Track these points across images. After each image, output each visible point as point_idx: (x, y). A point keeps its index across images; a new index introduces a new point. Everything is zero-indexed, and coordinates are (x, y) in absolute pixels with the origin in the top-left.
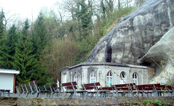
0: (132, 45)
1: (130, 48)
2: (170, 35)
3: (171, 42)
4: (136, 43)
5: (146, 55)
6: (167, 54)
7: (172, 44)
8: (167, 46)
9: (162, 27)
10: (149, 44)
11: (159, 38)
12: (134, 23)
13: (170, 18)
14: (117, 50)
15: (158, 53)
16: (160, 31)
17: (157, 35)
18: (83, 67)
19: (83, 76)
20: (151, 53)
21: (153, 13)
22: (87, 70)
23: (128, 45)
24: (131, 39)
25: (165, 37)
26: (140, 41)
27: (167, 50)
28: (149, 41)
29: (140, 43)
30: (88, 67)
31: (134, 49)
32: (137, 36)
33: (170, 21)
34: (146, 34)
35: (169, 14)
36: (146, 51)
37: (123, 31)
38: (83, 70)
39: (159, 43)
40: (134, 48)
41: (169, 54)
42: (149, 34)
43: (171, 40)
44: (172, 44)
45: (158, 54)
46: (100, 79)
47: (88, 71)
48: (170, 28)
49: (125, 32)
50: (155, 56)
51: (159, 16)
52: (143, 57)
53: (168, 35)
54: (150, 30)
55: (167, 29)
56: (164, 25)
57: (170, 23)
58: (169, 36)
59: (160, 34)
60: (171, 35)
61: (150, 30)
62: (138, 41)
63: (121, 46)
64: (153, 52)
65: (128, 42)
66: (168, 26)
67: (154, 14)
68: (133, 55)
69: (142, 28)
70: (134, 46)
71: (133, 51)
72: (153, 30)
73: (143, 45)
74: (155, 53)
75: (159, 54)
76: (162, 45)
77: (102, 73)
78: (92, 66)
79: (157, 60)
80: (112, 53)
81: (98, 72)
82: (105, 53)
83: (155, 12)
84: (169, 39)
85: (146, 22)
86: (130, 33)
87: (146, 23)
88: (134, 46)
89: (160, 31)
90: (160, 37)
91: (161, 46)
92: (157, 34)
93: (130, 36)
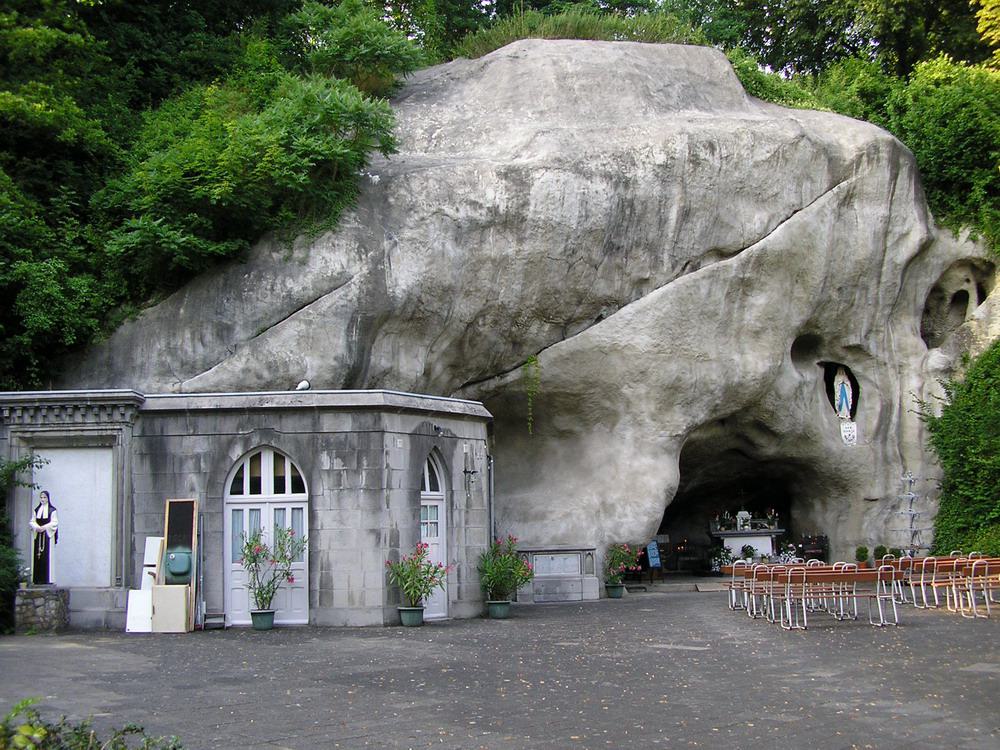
0: (482, 314)
1: (462, 326)
2: (660, 310)
3: (659, 345)
4: (503, 306)
5: (512, 376)
6: (626, 390)
7: (659, 352)
8: (637, 357)
9: (631, 263)
10: (547, 327)
11: (598, 309)
12: (533, 202)
13: (671, 235)
14: (404, 326)
15: (577, 380)
16: (617, 277)
17: (600, 295)
18: (387, 420)
19: (389, 487)
20: (547, 376)
21: (616, 185)
22: (408, 448)
23: (464, 308)
24: (493, 279)
25: (638, 312)
26: (528, 303)
27: (632, 374)
28: (557, 313)
29: (519, 314)
30: (414, 422)
31: (480, 334)
32: (527, 274)
33: (667, 247)
34: (566, 278)
35: (673, 215)
36: (520, 360)
37: (465, 226)
38: (388, 438)
39: (599, 333)
40: (481, 329)
41: (638, 397)
42: (576, 282)
43: (661, 333)
44: (659, 352)
45: (576, 384)
46: (468, 505)
47: (411, 450)
48: (660, 278)
49: (470, 230)
50: (555, 391)
51: (639, 208)
52: (492, 384)
53: (654, 306)
55: (646, 280)
56: (643, 256)
57: (666, 257)
58: (657, 313)
59: (609, 293)
60: (664, 310)
62: (522, 299)
63: (436, 305)
64: (556, 371)
65: (468, 294)
66: (656, 264)
67: (621, 189)
68: (453, 366)
69: (567, 240)
70: (489, 319)
71: (467, 345)
73: (526, 325)
74: (564, 376)
75: (582, 386)
76: (614, 349)
77: (477, 469)
78: (429, 419)
80: (378, 338)
81: (458, 466)
82: (349, 330)
83: (627, 184)
84: (654, 327)
85: (587, 217)
86: (497, 245)
87: (587, 225)
88: (489, 319)
89: (617, 277)
90: (608, 305)
91: (604, 352)
92: (602, 289)
93: (494, 261)
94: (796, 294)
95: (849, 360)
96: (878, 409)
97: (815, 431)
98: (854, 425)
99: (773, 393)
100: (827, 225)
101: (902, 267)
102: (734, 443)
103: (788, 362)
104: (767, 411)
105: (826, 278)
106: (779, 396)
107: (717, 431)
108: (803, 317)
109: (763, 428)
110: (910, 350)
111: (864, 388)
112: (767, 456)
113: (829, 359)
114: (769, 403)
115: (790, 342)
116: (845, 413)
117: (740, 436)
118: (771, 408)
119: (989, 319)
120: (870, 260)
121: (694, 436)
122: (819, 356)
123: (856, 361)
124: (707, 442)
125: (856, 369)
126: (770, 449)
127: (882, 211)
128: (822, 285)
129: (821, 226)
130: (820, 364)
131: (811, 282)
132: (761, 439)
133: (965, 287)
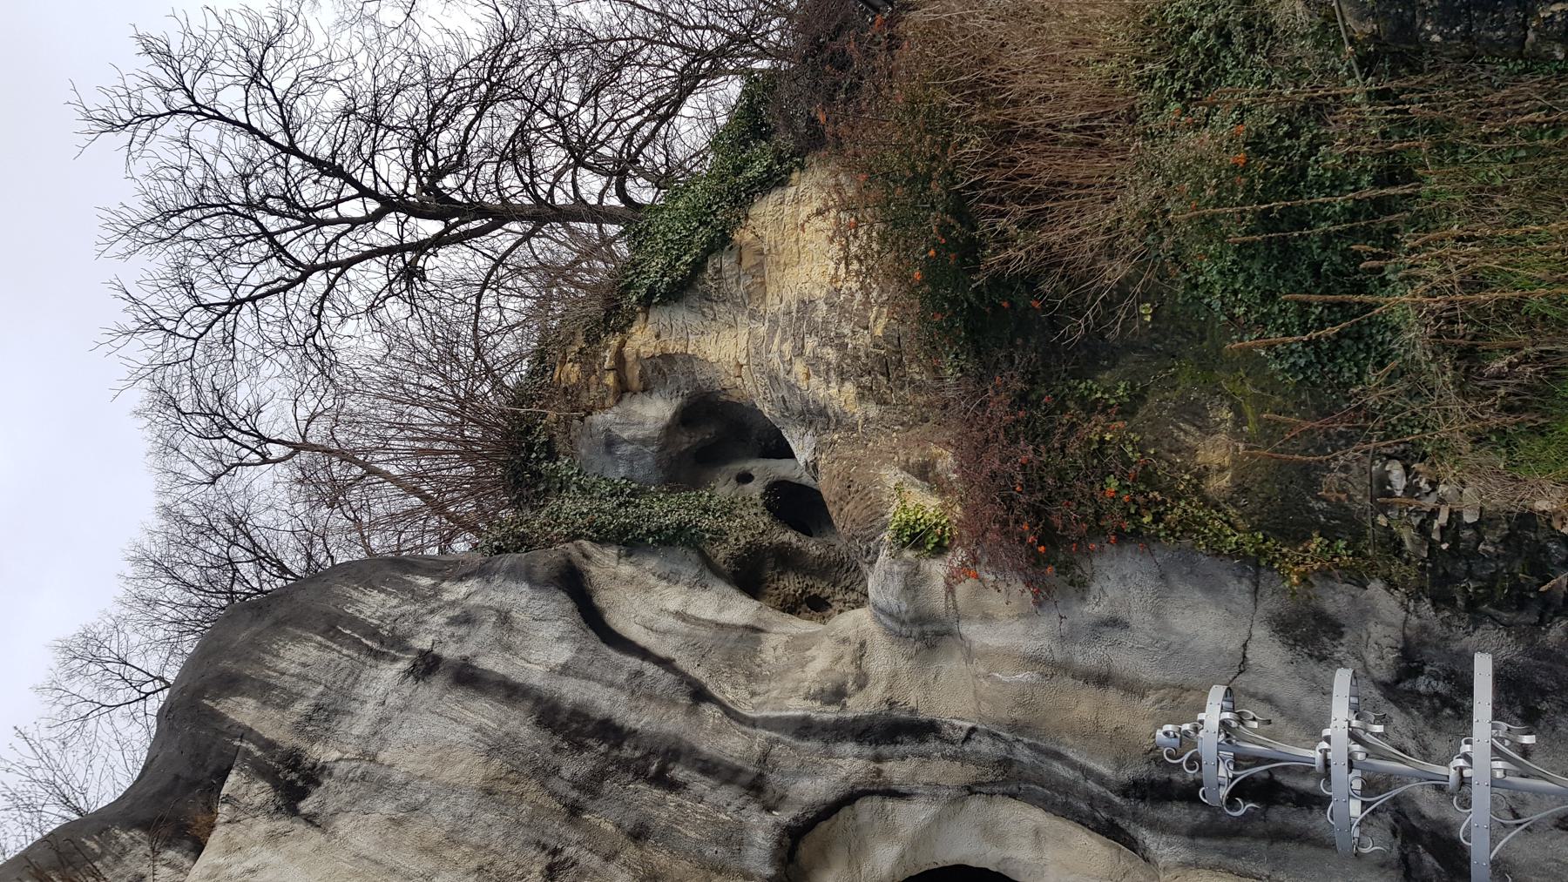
101: (593, 641)
119: (816, 417)
133: (755, 489)
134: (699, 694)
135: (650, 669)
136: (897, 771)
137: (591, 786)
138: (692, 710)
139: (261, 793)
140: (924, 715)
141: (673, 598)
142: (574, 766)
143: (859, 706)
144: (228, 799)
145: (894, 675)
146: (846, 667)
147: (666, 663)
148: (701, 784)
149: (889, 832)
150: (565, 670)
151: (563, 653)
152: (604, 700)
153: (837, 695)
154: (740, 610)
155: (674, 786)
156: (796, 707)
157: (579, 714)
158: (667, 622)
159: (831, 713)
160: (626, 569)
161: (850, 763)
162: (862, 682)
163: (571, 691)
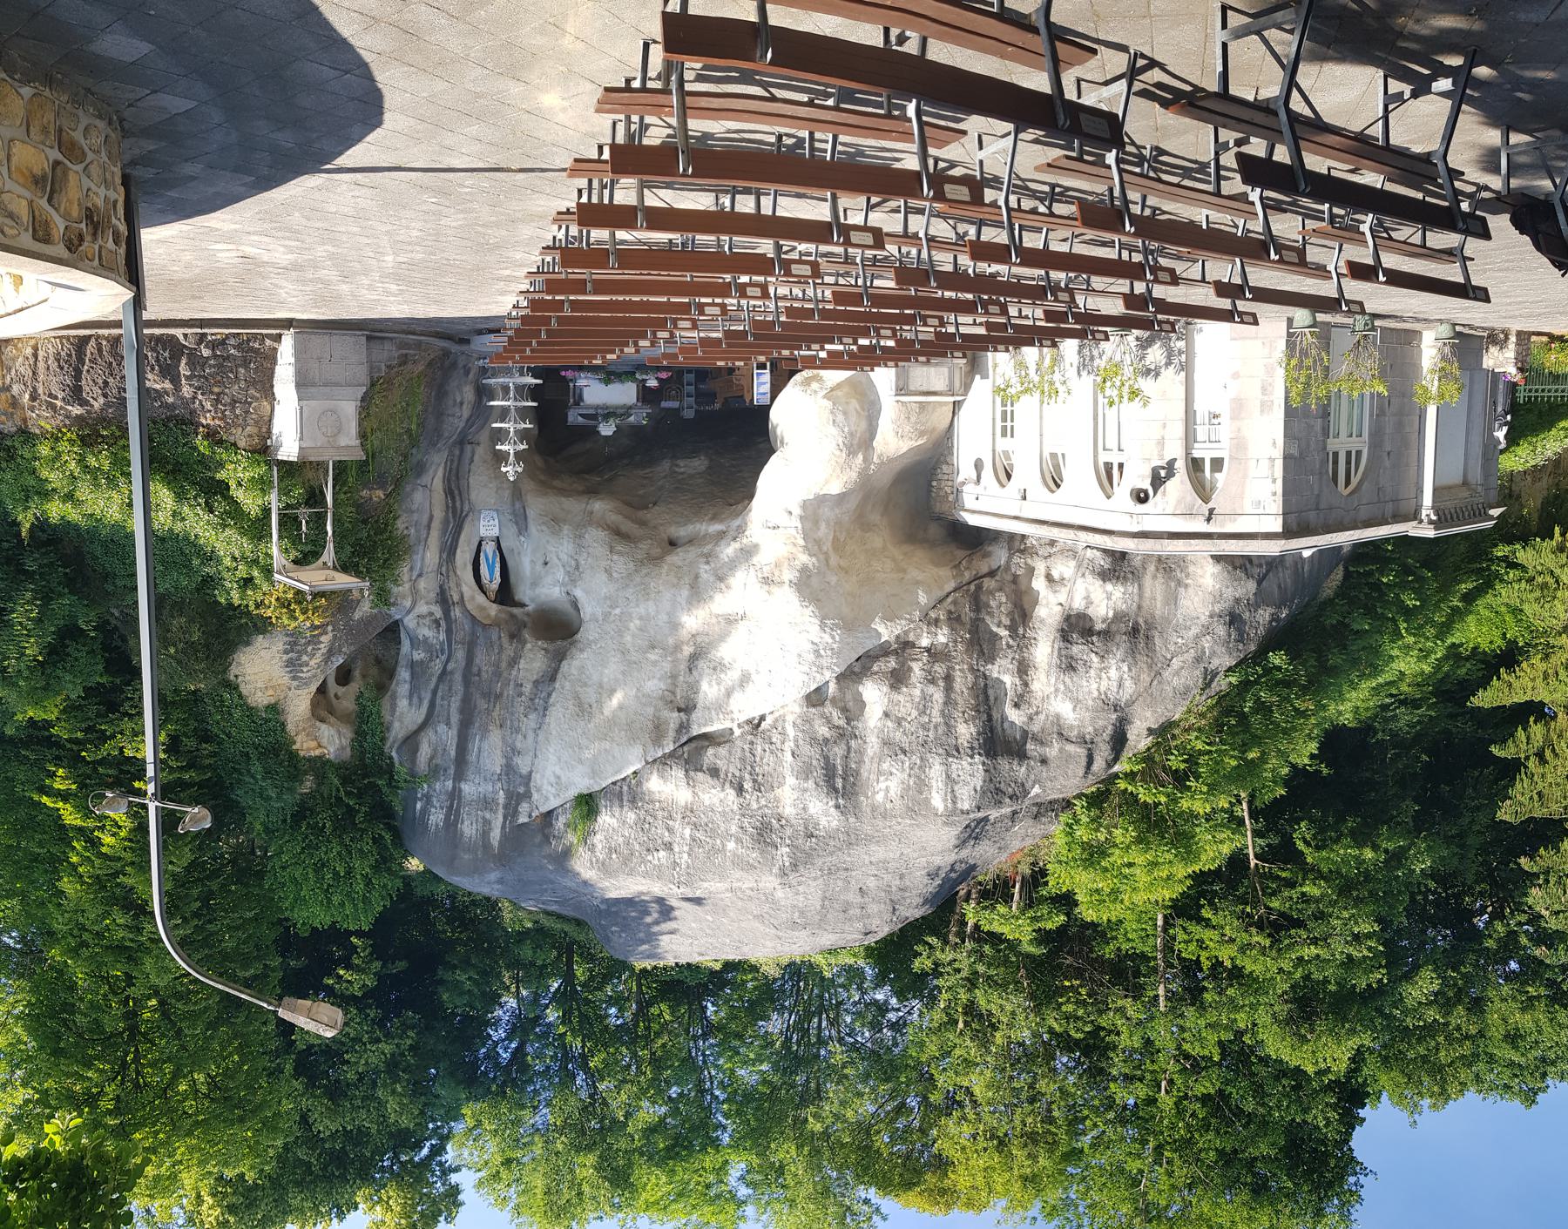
54: (899, 722)
61: (899, 722)
72: (886, 715)
79: (905, 554)
94: (591, 691)
95: (493, 609)
96: (458, 551)
97: (544, 528)
98: (483, 532)
99: (615, 575)
100: (548, 773)
102: (641, 514)
103: (588, 609)
104: (620, 554)
105: (545, 709)
106: (608, 571)
107: (682, 532)
108: (576, 663)
109: (618, 533)
110: (427, 621)
111: (467, 575)
112: (602, 499)
113: (516, 611)
114: (621, 565)
115: (588, 632)
116: (489, 548)
117: (643, 523)
118: (615, 557)
120: (485, 732)
121: (716, 527)
122: (528, 614)
123: (482, 608)
124: (688, 521)
125: (481, 598)
126: (599, 506)
127: (466, 788)
128: (551, 700)
129: (558, 772)
130: (523, 605)
131: (570, 704)
132: (614, 518)
134: (444, 672)
135: (440, 694)
136: (456, 598)
137: (487, 695)
138: (452, 673)
139: (524, 807)
140: (438, 590)
141: (403, 703)
142: (482, 704)
143: (438, 613)
144: (530, 816)
145: (427, 603)
146: (427, 621)
147: (435, 692)
148: (477, 661)
149: (473, 598)
150: (448, 724)
151: (442, 728)
152: (455, 703)
153: (437, 622)
154: (404, 674)
155: (480, 670)
156: (442, 636)
157: (462, 711)
158: (415, 700)
159: (443, 623)
160: (396, 725)
161: (457, 612)
162: (431, 614)
163: (455, 718)
